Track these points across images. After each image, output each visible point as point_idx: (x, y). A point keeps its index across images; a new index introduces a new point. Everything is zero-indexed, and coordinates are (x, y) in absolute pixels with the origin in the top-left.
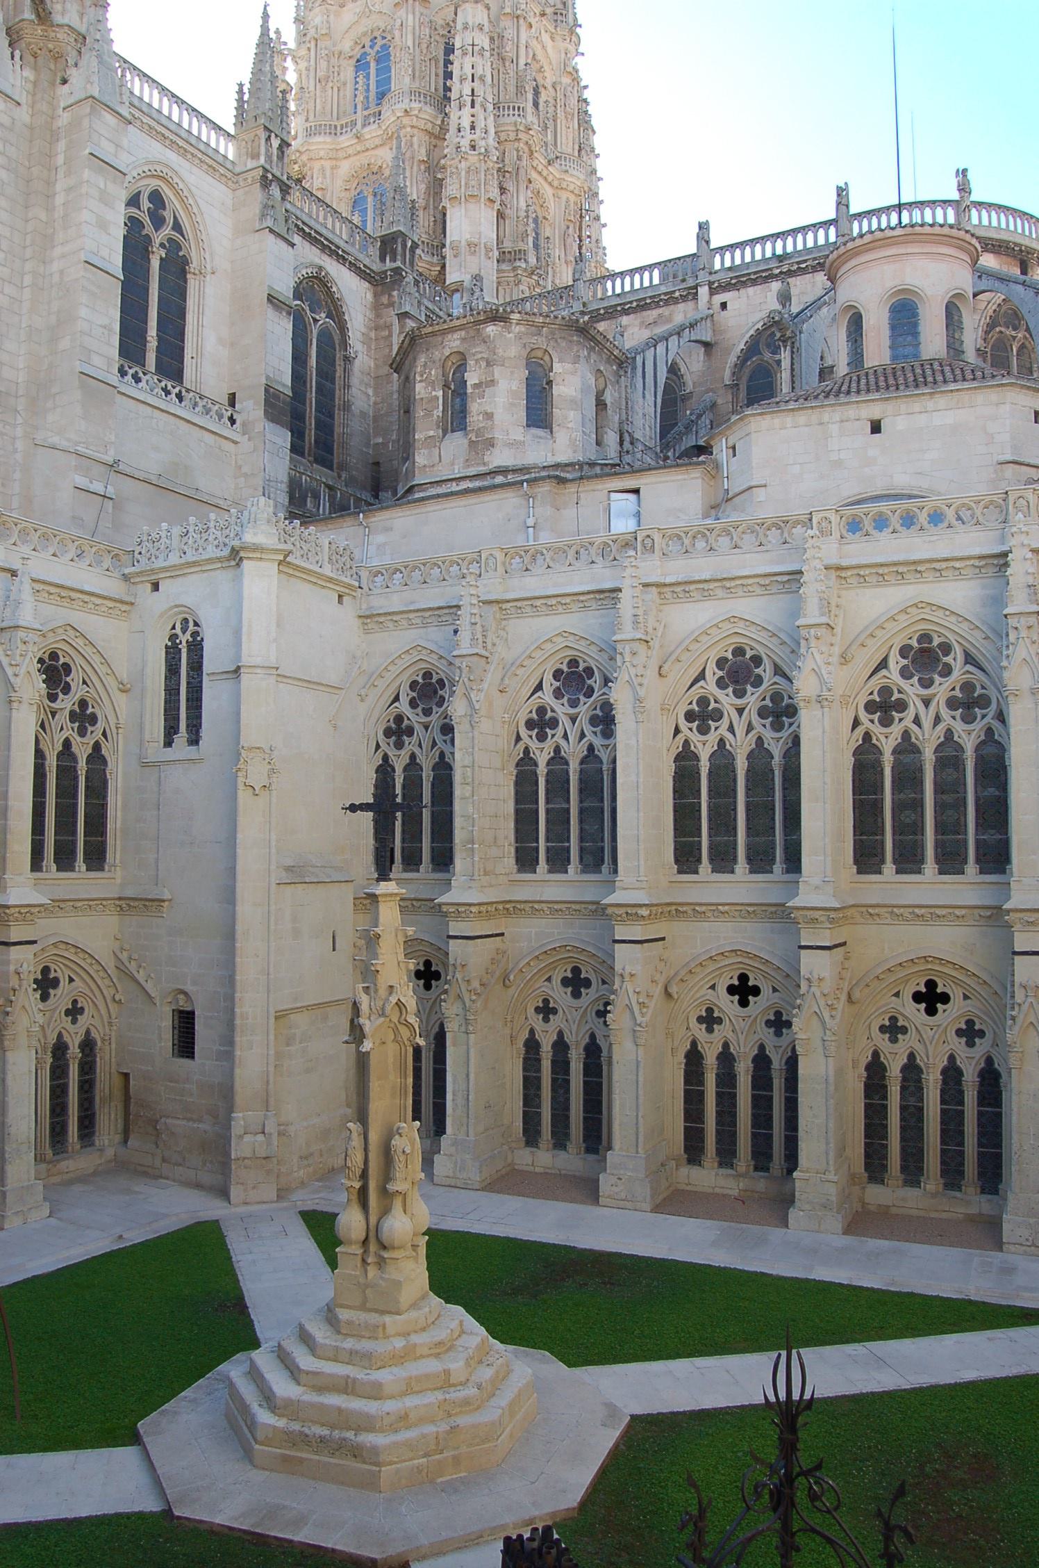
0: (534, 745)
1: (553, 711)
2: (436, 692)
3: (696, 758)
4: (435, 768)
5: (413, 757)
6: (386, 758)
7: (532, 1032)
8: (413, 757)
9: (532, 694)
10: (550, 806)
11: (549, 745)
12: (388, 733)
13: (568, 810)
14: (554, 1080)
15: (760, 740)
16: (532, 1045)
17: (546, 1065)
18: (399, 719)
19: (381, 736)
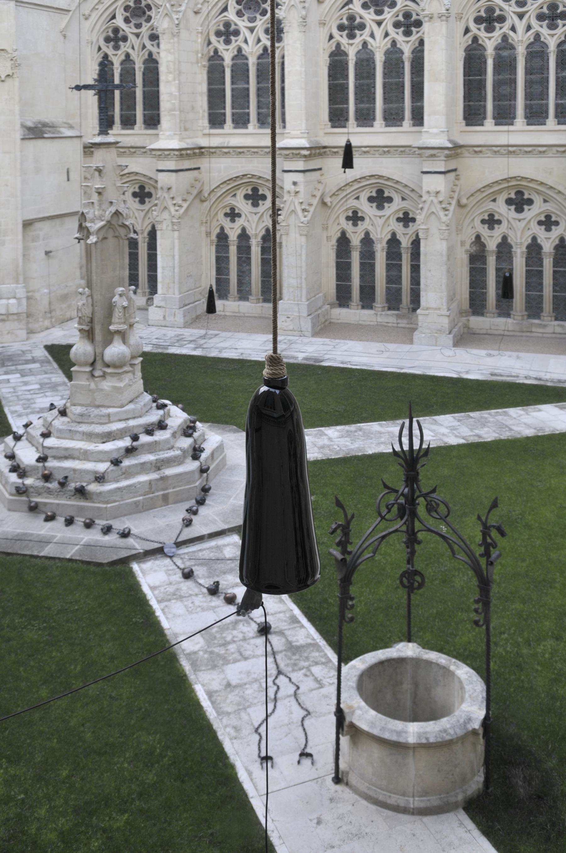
0: (221, 47)
1: (236, 25)
2: (144, 13)
3: (346, 54)
4: (145, 62)
5: (128, 55)
6: (106, 56)
7: (222, 229)
8: (128, 55)
9: (220, 14)
10: (235, 86)
11: (233, 47)
12: (107, 40)
13: (248, 89)
14: (239, 259)
15: (394, 43)
16: (222, 237)
17: (233, 250)
18: (116, 30)
19: (102, 43)
